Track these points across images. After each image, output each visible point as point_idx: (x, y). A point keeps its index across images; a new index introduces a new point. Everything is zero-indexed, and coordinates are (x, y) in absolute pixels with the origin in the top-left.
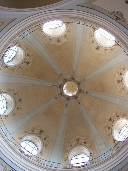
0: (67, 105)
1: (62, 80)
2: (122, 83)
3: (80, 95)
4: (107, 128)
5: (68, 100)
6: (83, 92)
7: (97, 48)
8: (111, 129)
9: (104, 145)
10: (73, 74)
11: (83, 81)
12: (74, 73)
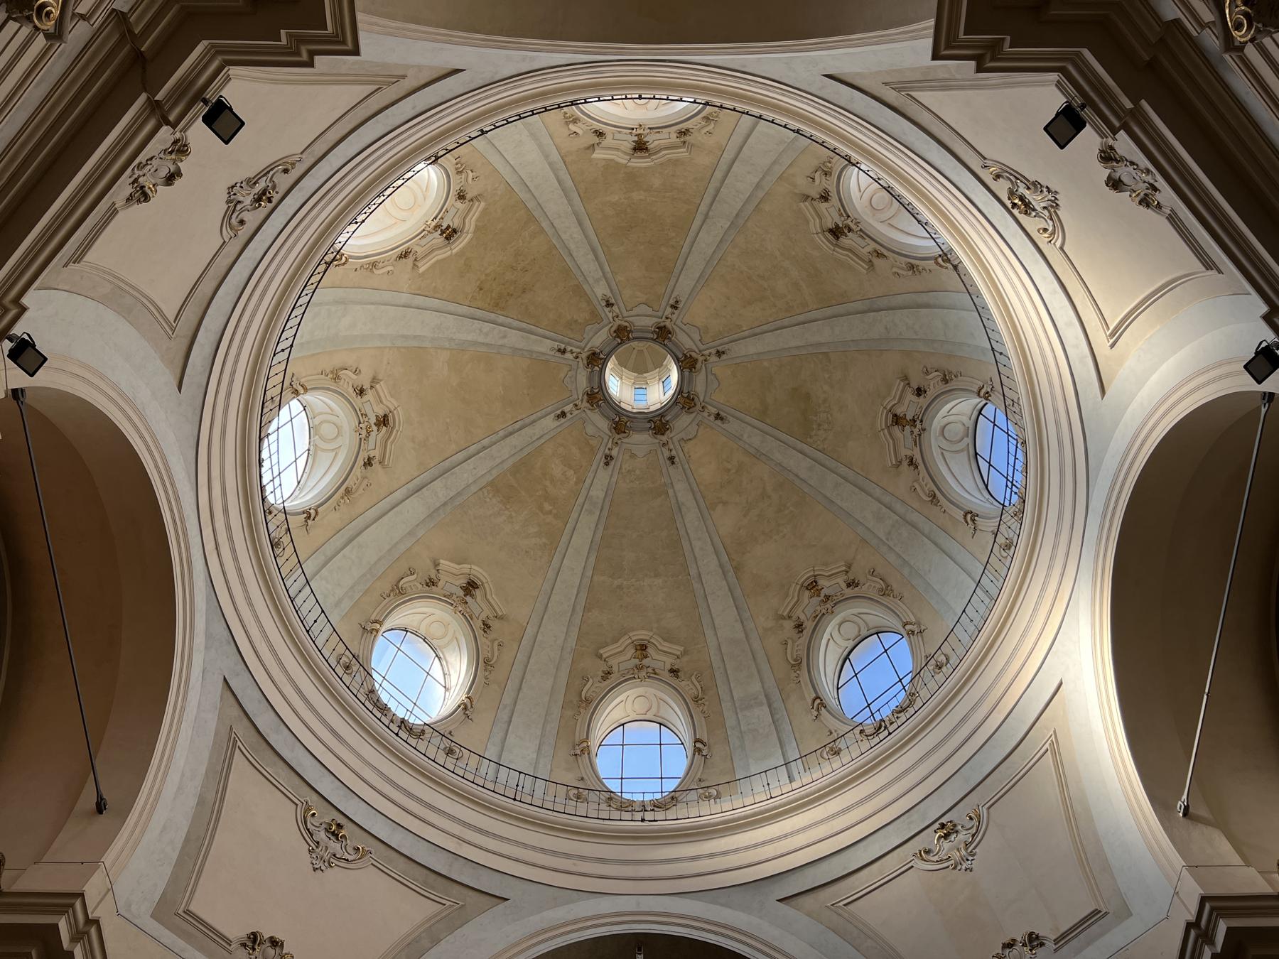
0: (612, 458)
1: (607, 328)
3: (682, 423)
4: (789, 625)
6: (698, 407)
7: (836, 232)
8: (807, 633)
9: (766, 708)
10: (669, 310)
11: (714, 358)
12: (674, 307)
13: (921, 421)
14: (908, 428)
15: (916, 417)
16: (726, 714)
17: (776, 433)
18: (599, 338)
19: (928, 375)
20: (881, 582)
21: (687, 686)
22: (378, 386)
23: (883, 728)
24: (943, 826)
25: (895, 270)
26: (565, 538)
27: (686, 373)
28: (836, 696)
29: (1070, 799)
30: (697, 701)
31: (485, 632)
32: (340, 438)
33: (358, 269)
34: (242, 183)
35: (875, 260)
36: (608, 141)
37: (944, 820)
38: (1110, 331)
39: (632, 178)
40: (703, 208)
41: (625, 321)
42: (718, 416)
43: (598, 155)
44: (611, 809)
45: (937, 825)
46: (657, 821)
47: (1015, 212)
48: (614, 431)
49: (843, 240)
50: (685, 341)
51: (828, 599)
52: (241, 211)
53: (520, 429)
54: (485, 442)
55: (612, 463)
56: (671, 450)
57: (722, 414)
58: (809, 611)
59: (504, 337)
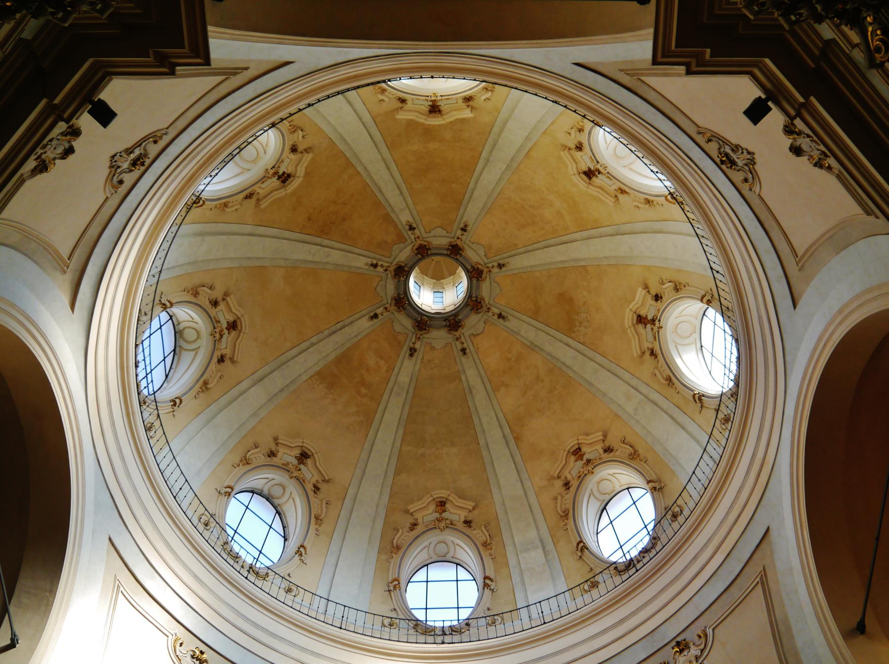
0: (415, 350)
1: (410, 247)
2: (652, 329)
3: (473, 322)
4: (559, 483)
5: (420, 331)
6: (484, 309)
7: (589, 174)
8: (573, 490)
9: (540, 551)
10: (459, 232)
11: (496, 270)
12: (464, 229)
13: (659, 321)
14: (649, 326)
15: (655, 317)
16: (509, 556)
17: (548, 329)
18: (404, 254)
19: (663, 285)
20: (631, 449)
21: (480, 535)
22: (228, 299)
23: (632, 565)
24: (678, 644)
25: (636, 204)
26: (378, 416)
27: (474, 281)
28: (596, 540)
29: (776, 621)
30: (486, 546)
31: (315, 493)
32: (199, 340)
33: (213, 209)
34: (121, 153)
35: (621, 197)
36: (409, 105)
37: (679, 639)
38: (798, 258)
39: (428, 133)
40: (484, 154)
41: (425, 241)
42: (500, 316)
43: (402, 116)
44: (418, 633)
45: (674, 643)
46: (454, 643)
47: (724, 167)
48: (416, 328)
49: (594, 179)
50: (473, 255)
51: (589, 462)
52: (121, 173)
53: (341, 329)
54: (314, 340)
55: (416, 354)
56: (463, 343)
57: (504, 314)
58: (575, 473)
59: (329, 255)
